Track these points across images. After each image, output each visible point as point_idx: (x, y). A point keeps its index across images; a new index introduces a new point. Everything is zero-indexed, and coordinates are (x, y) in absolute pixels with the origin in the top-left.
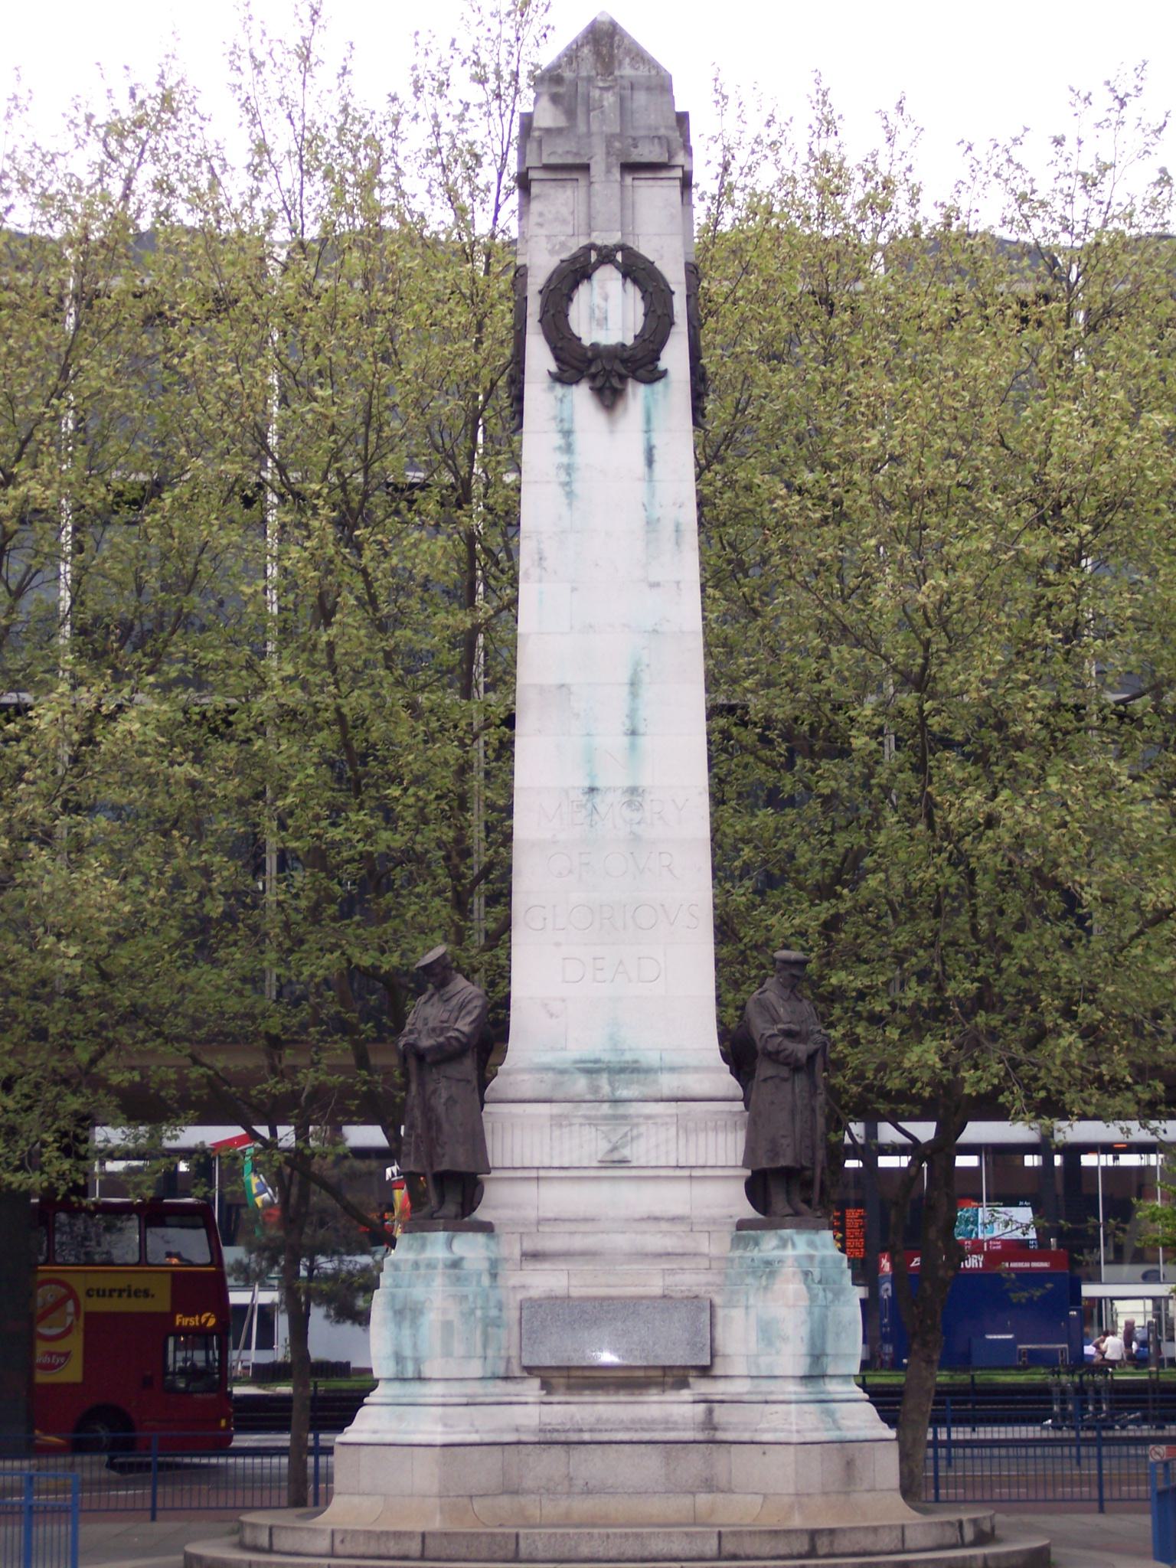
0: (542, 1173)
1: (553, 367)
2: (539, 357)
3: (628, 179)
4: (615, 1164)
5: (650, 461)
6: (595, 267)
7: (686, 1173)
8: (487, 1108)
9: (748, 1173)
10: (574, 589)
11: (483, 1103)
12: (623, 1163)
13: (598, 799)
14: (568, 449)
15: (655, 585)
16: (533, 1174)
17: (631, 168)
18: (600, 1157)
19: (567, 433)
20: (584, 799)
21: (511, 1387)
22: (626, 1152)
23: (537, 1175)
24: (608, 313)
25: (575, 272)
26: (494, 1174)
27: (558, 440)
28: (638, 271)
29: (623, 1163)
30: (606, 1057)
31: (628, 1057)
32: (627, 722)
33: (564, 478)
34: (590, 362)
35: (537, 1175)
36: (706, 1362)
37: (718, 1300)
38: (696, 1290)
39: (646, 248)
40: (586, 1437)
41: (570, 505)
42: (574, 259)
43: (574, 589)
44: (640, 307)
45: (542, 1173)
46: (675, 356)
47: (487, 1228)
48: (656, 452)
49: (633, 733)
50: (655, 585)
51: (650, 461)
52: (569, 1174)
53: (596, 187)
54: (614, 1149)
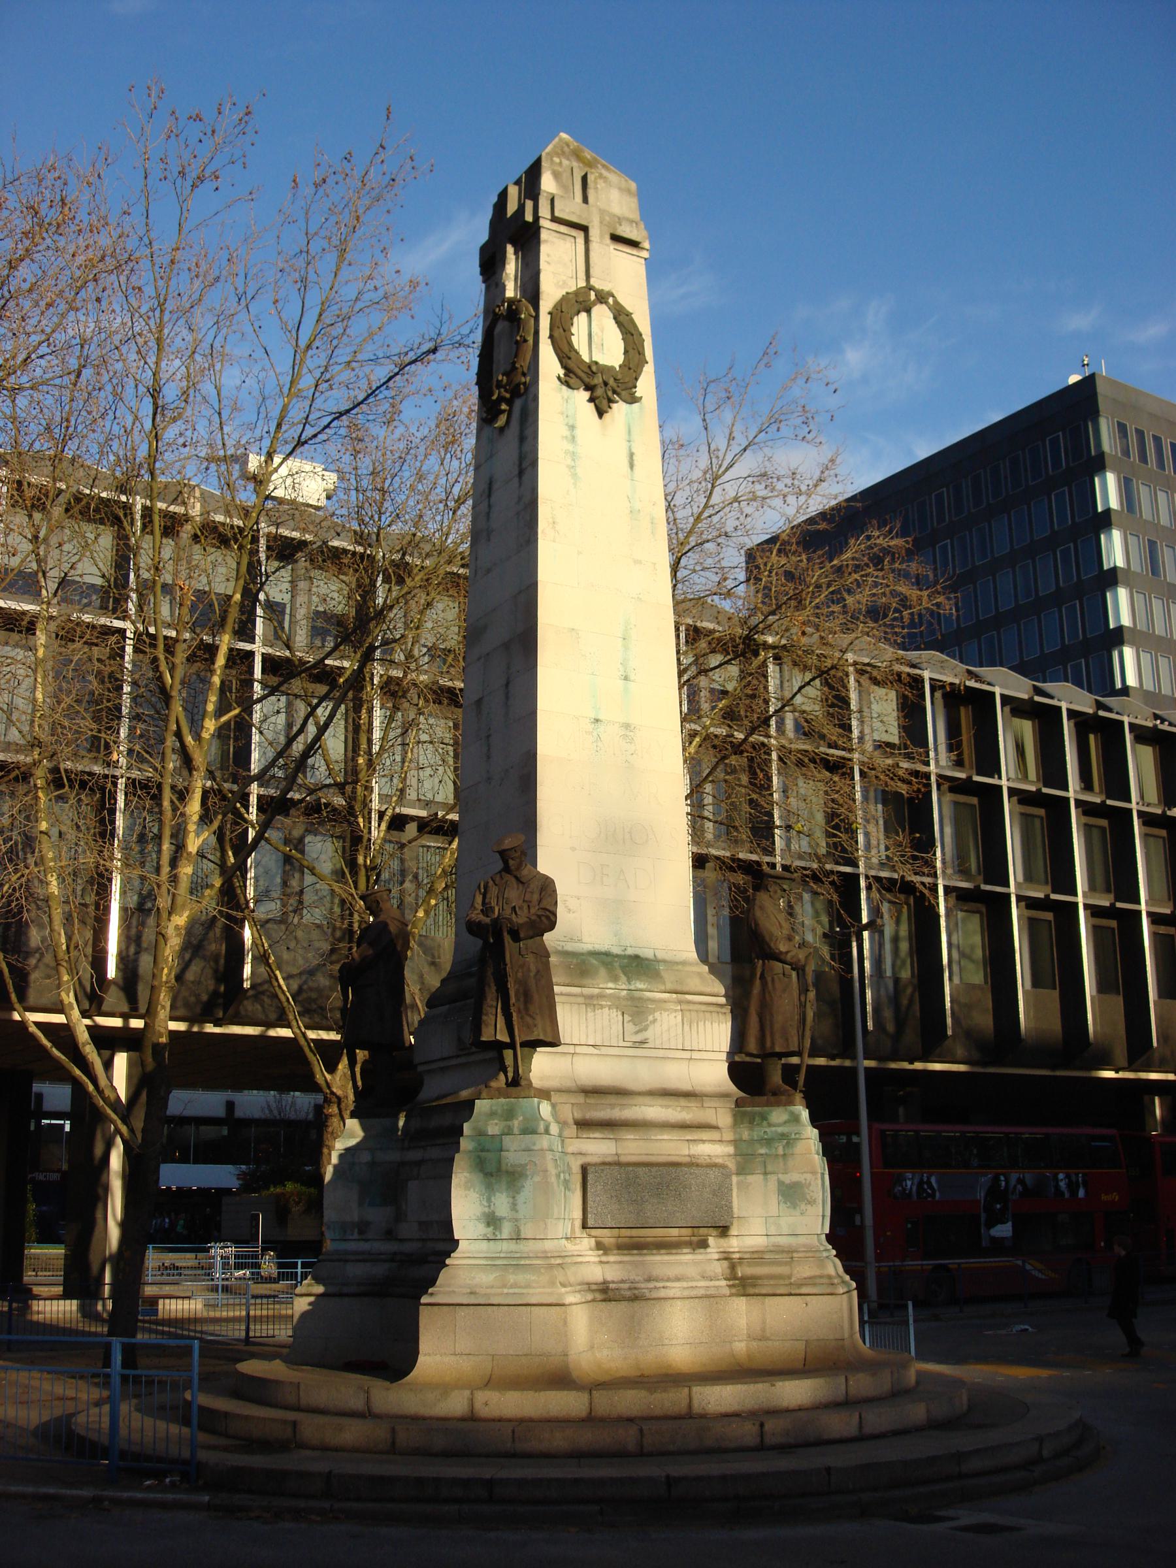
1: (562, 372)
3: (613, 246)
5: (632, 466)
6: (594, 304)
7: (687, 1055)
10: (579, 553)
13: (601, 728)
14: (573, 439)
15: (637, 562)
17: (616, 238)
19: (572, 427)
20: (590, 727)
25: (581, 301)
27: (567, 433)
28: (623, 319)
30: (616, 950)
31: (630, 952)
32: (622, 669)
33: (569, 462)
39: (627, 303)
41: (575, 484)
42: (577, 293)
43: (579, 553)
44: (621, 346)
46: (646, 385)
48: (635, 458)
49: (626, 678)
50: (637, 562)
51: (632, 466)
53: (594, 246)
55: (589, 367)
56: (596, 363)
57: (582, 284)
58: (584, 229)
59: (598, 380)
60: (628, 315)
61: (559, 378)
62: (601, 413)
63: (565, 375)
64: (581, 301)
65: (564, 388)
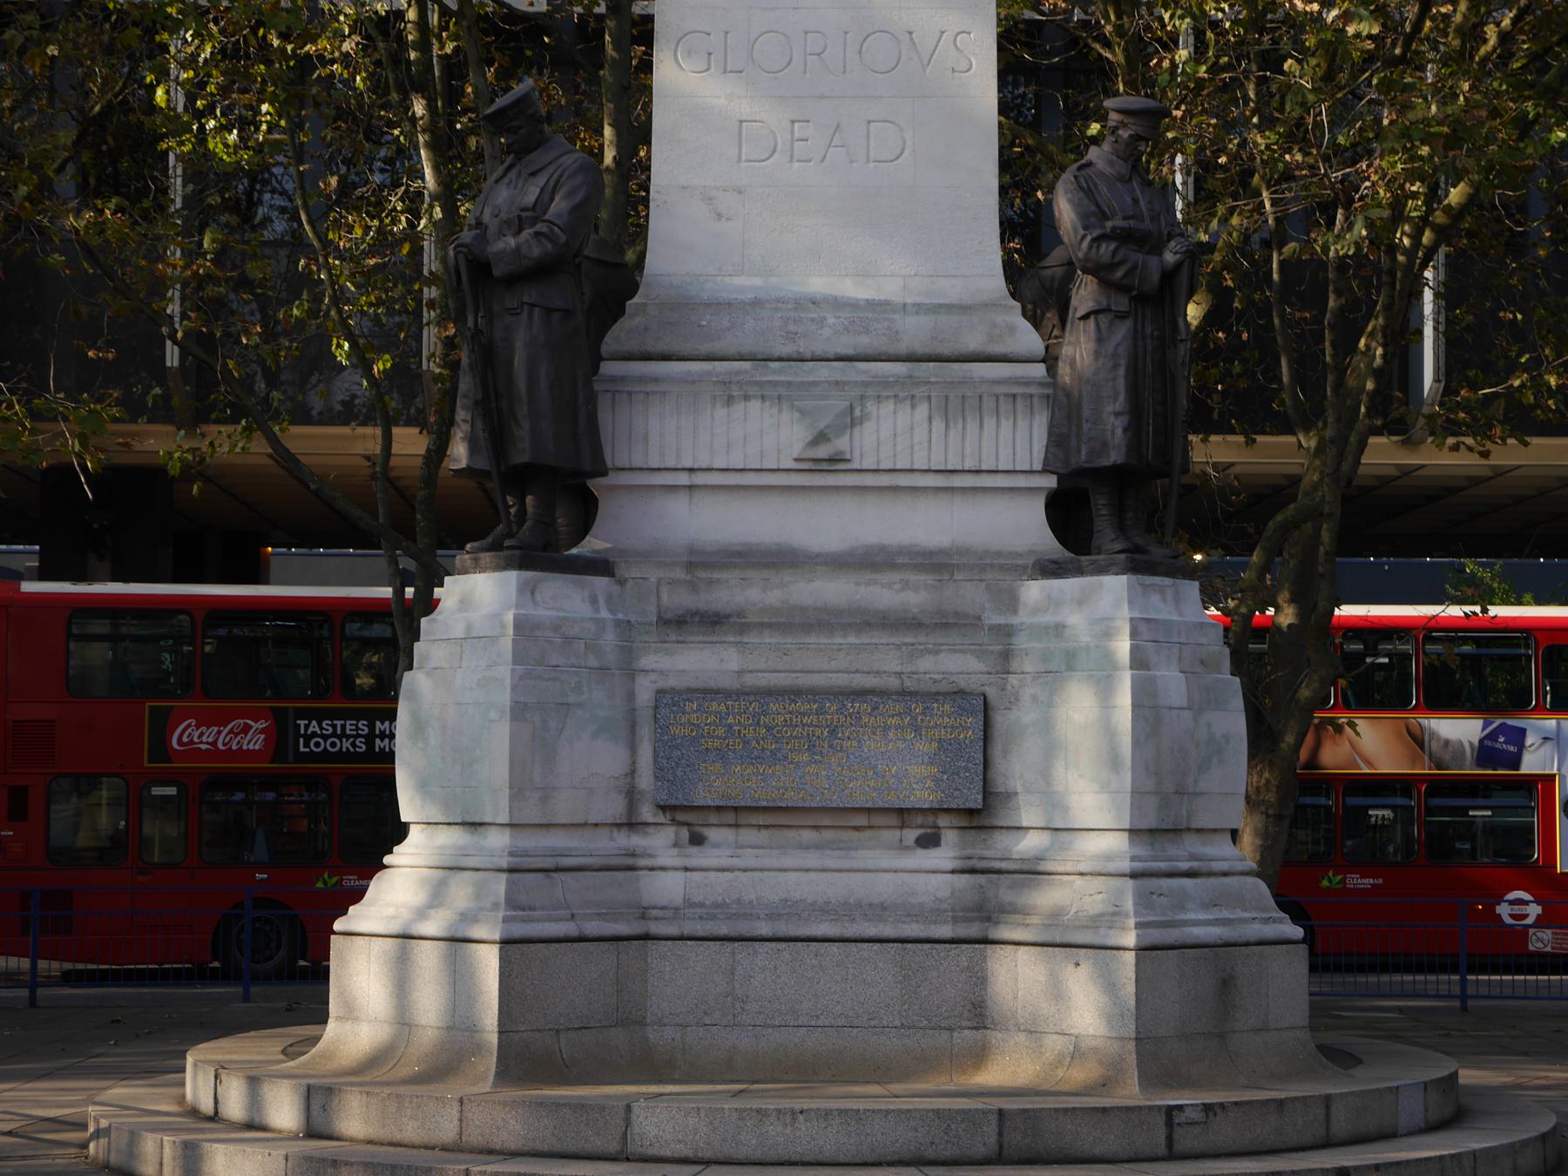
0: (700, 479)
4: (825, 465)
8: (608, 368)
9: (1051, 482)
11: (597, 359)
12: (835, 462)
16: (683, 479)
18: (797, 450)
21: (636, 841)
22: (841, 444)
23: (694, 483)
26: (613, 479)
29: (835, 462)
35: (694, 483)
36: (976, 801)
37: (992, 693)
38: (962, 683)
40: (764, 929)
45: (700, 479)
47: (600, 566)
52: (742, 484)
54: (820, 438)
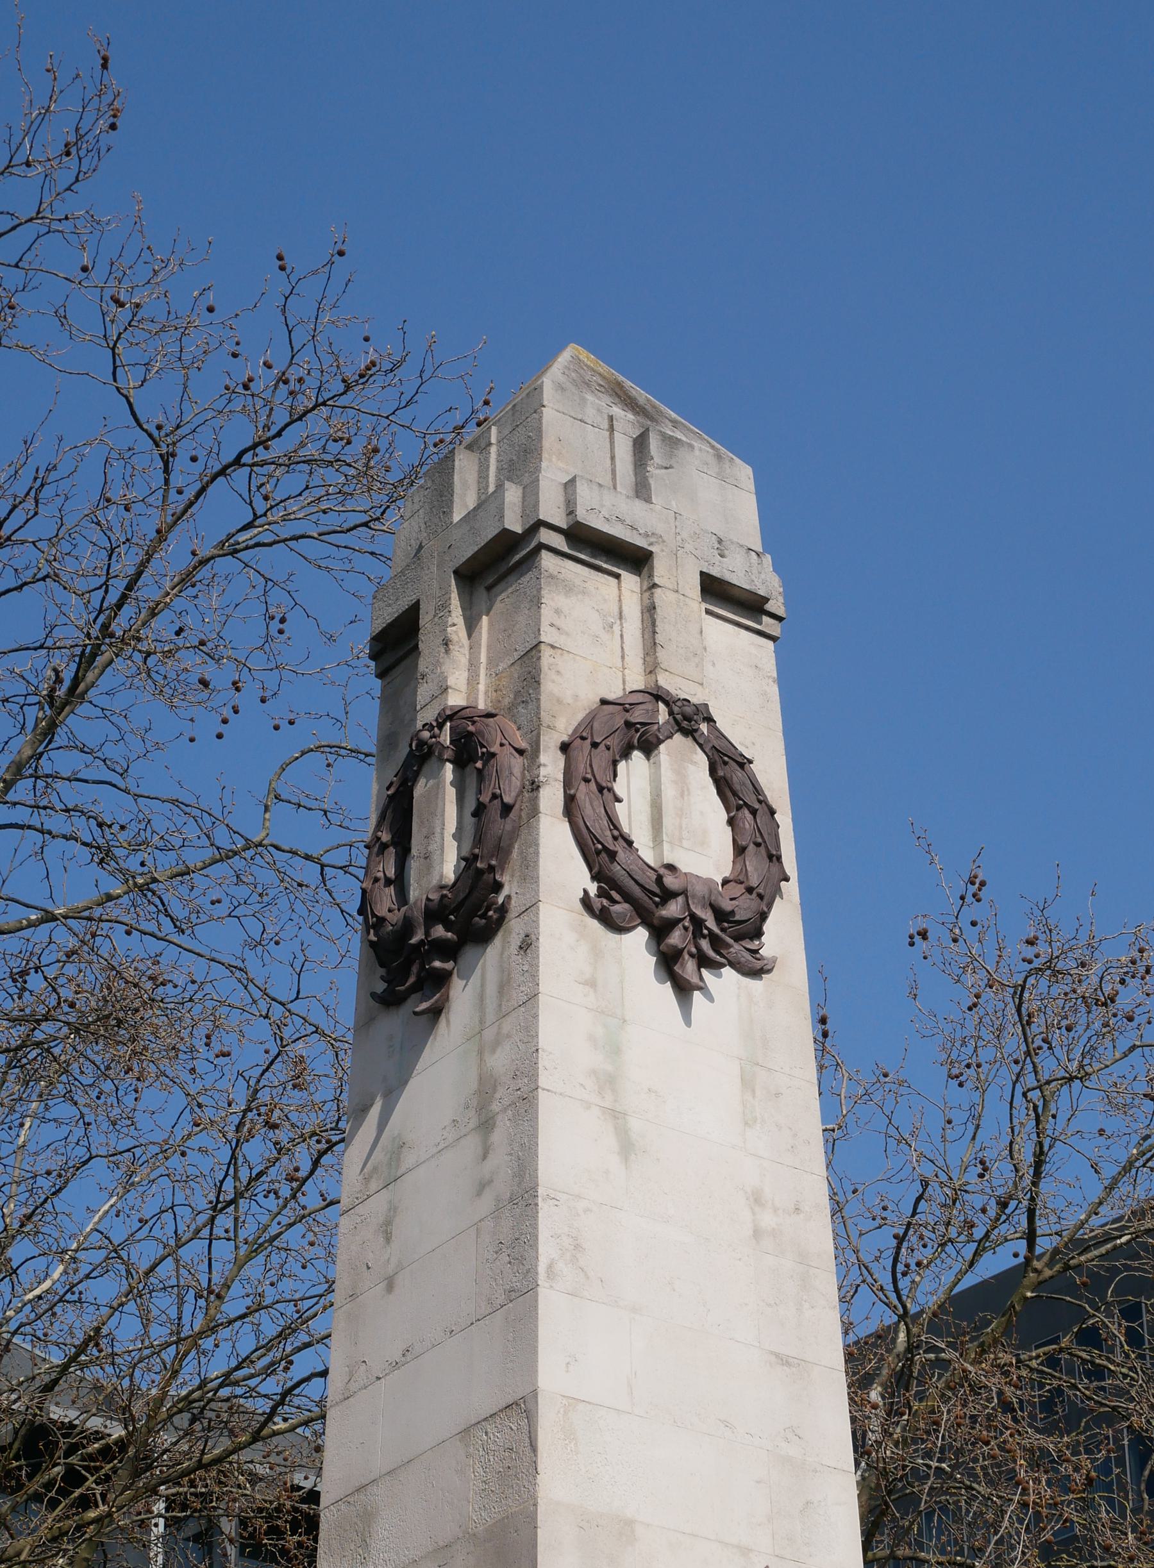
1: (593, 888)
2: (557, 870)
14: (615, 1050)
24: (678, 822)
28: (728, 771)
34: (668, 895)
46: (783, 933)
55: (659, 880)
56: (671, 868)
57: (637, 680)
58: (635, 559)
59: (673, 909)
60: (743, 763)
61: (586, 902)
62: (683, 989)
63: (601, 893)
64: (636, 726)
65: (594, 924)
